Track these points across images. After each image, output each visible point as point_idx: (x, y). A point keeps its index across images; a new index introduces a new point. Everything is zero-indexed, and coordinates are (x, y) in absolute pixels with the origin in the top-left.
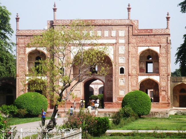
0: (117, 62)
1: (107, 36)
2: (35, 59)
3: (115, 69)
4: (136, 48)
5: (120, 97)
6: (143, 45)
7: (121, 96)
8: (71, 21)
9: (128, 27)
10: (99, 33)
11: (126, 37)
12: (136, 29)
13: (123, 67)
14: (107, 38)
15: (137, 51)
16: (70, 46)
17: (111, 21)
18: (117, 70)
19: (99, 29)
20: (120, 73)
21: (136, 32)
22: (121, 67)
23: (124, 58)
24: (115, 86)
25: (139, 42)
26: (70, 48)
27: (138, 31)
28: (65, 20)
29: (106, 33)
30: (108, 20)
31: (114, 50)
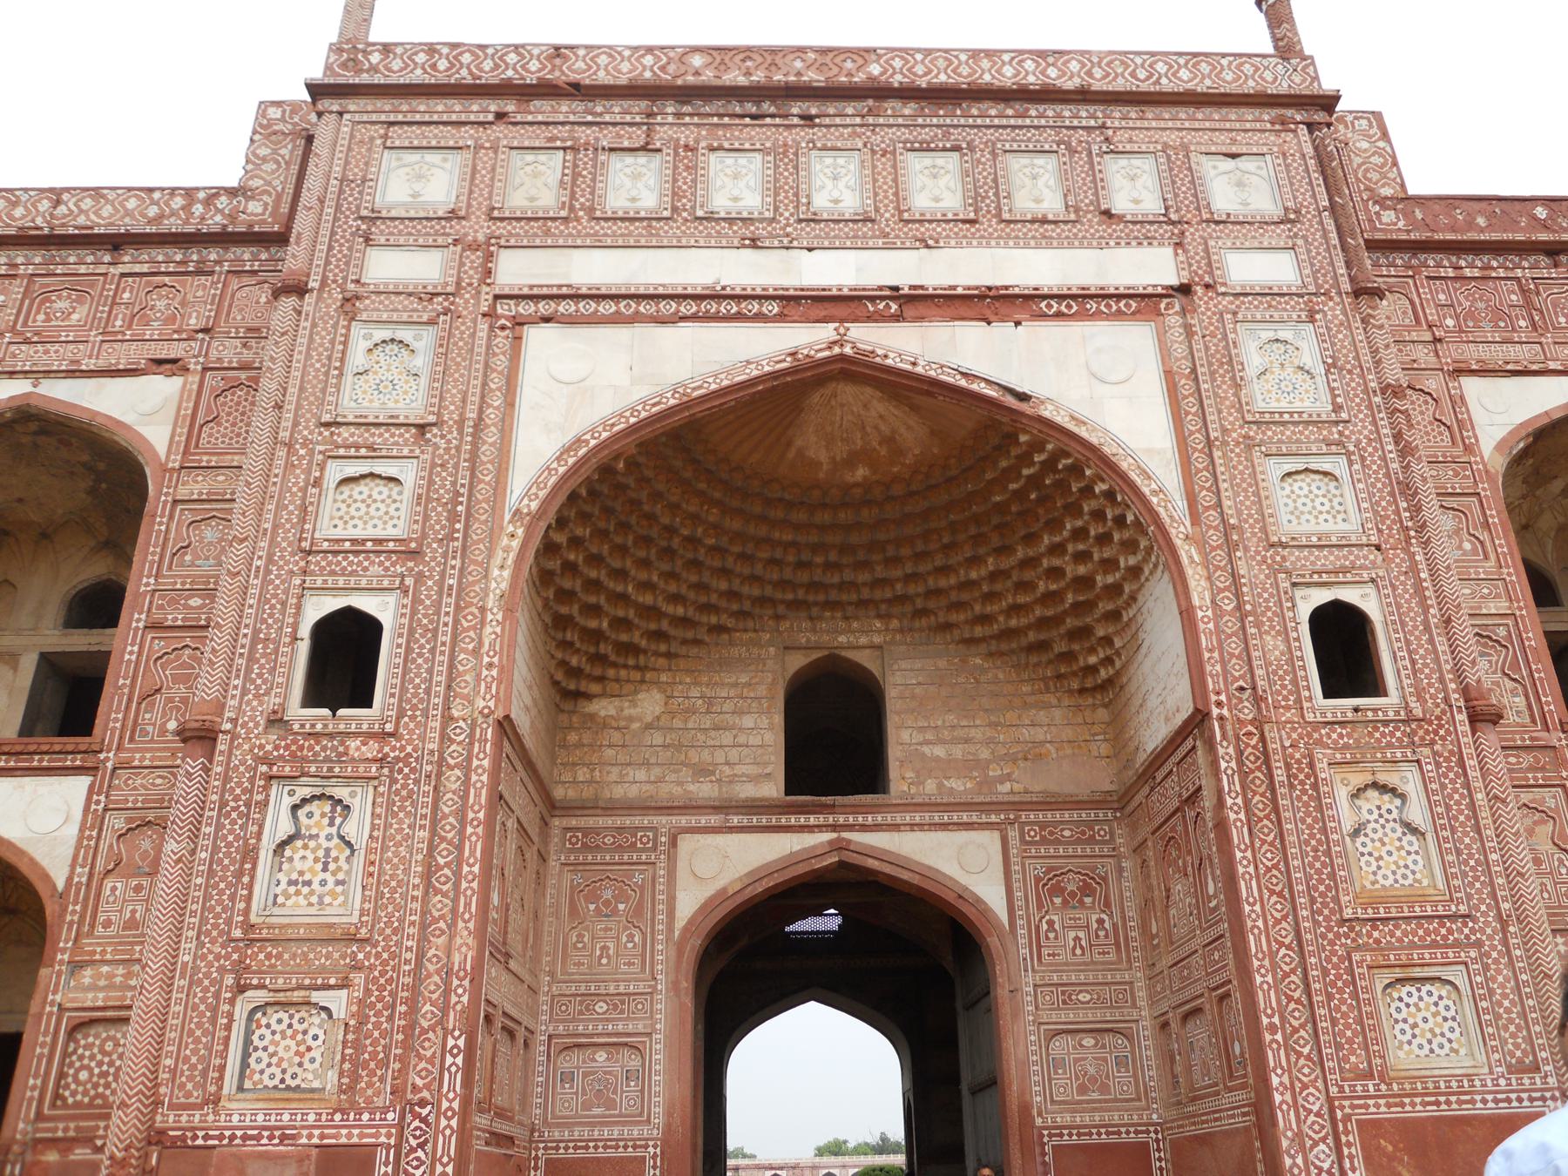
0: (1251, 532)
1: (1052, 204)
2: (54, 611)
3: (1231, 625)
4: (1433, 383)
5: (1418, 1110)
6: (1521, 354)
7: (1432, 1090)
8: (558, 51)
9: (1311, 126)
10: (935, 184)
11: (1309, 225)
12: (1387, 192)
13: (1350, 595)
14: (1043, 229)
15: (1459, 427)
16: (519, 322)
17: (1074, 66)
18: (1274, 644)
19: (926, 134)
20: (1326, 695)
21: (1388, 216)
22: (1322, 597)
23: (1338, 465)
24: (1276, 908)
25: (1450, 322)
26: (518, 338)
27: (1408, 215)
28: (483, 47)
29: (1036, 184)
30: (1042, 54)
31: (1169, 375)
